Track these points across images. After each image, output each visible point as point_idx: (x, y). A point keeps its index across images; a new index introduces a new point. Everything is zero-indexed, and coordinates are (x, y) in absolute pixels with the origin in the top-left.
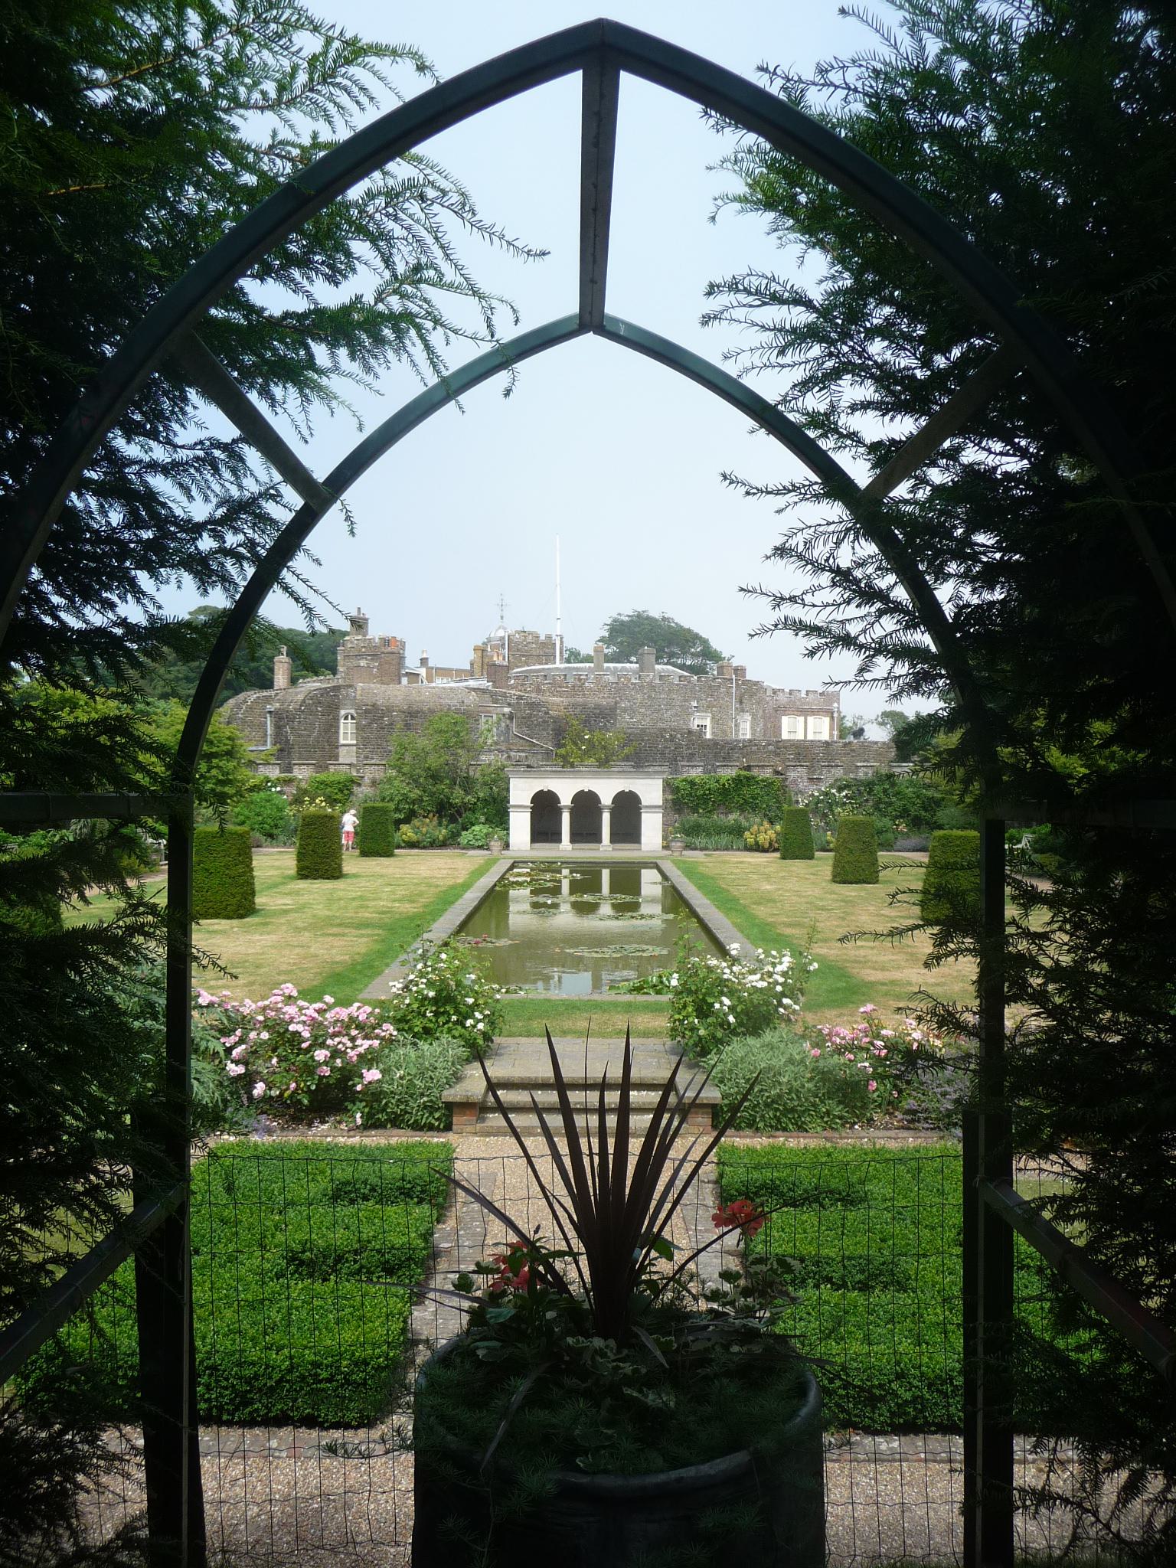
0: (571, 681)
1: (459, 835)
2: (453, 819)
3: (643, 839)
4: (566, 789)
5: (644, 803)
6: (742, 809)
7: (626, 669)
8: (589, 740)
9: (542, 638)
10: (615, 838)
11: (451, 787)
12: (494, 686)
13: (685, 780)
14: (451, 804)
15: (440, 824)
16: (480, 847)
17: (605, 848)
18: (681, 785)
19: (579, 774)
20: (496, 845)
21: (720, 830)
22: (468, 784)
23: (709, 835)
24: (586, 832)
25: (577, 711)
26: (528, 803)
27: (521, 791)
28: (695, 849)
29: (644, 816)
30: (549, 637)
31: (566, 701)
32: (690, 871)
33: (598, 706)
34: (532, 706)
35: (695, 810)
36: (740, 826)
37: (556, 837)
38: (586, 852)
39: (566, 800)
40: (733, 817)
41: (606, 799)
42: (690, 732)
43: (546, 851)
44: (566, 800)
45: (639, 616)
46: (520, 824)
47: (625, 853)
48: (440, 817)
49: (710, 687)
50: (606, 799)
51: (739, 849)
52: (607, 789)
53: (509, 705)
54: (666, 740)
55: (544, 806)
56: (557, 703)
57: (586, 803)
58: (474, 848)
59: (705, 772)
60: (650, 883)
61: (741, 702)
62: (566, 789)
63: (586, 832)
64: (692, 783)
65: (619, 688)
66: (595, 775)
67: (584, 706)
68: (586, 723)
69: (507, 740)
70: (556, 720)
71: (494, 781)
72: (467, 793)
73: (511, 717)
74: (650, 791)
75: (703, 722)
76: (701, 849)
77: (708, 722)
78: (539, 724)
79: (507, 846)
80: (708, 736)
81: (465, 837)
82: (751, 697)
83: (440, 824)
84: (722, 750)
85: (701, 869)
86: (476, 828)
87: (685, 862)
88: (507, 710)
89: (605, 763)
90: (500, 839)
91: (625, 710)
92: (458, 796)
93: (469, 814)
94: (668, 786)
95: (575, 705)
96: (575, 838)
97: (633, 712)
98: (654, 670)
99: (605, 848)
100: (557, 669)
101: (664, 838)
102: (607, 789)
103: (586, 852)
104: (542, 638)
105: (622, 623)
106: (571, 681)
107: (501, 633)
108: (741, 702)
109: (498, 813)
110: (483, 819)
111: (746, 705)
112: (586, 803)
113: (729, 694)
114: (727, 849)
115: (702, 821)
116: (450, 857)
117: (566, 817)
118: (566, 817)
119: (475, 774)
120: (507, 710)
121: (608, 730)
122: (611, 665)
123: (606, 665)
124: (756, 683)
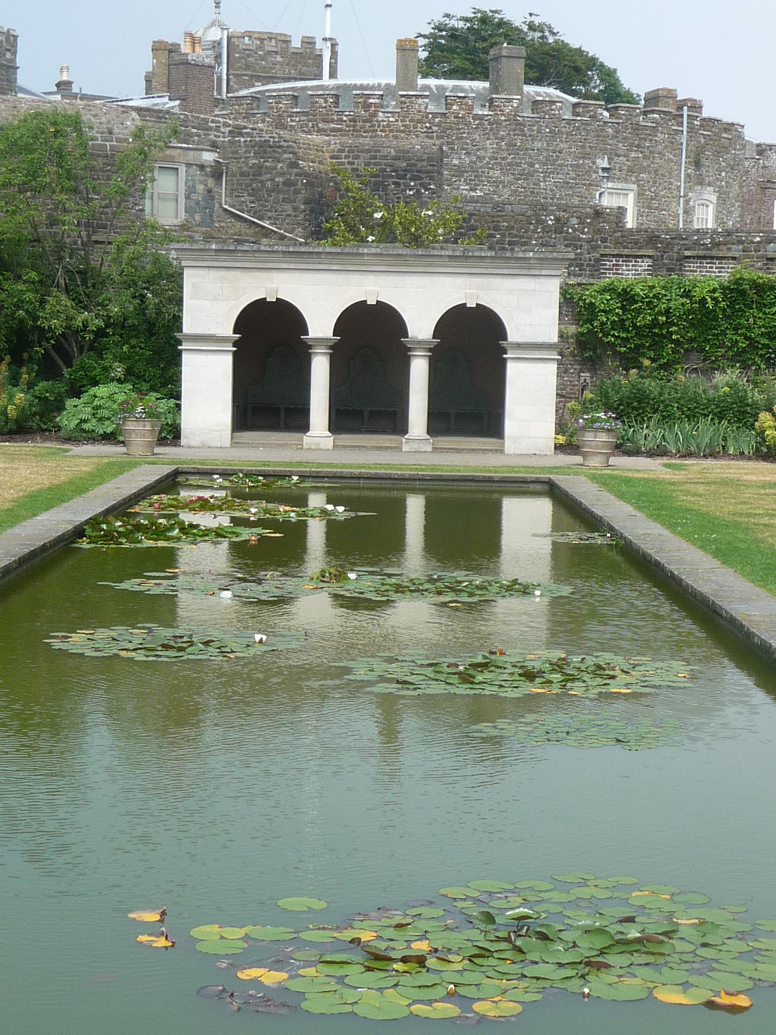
0: (348, 109)
1: (60, 408)
2: (48, 370)
3: (510, 426)
4: (321, 299)
5: (514, 334)
6: (741, 359)
7: (462, 90)
8: (385, 224)
9: (296, 43)
10: (439, 423)
11: (44, 285)
12: (182, 107)
13: (610, 289)
14: (41, 330)
15: (14, 380)
16: (109, 438)
17: (416, 445)
18: (601, 301)
19: (348, 262)
20: (140, 431)
21: (693, 410)
22: (85, 285)
23: (667, 418)
24: (368, 404)
25: (360, 164)
26: (227, 329)
27: (211, 302)
28: (636, 453)
29: (512, 369)
30: (309, 42)
31: (335, 142)
32: (653, 501)
33: (402, 154)
34: (263, 149)
35: (629, 361)
36: (742, 400)
37: (298, 420)
38: (368, 454)
39: (321, 324)
40: (726, 380)
41: (421, 325)
42: (598, 213)
43: (268, 450)
44: (321, 324)
45: (485, 20)
46: (207, 386)
47: (465, 457)
48: (17, 362)
49: (637, 127)
50: (421, 325)
51: (741, 455)
52: (422, 301)
53: (214, 146)
54: (547, 229)
55: (268, 337)
56: (319, 148)
57: (370, 333)
58: (92, 438)
59: (655, 270)
60: (526, 527)
61: (697, 164)
62: (321, 299)
63: (368, 404)
64: (626, 297)
65: (451, 122)
66: (397, 264)
67: (374, 153)
68: (378, 185)
69: (209, 220)
70: (313, 180)
71: (150, 281)
72: (81, 305)
73: (217, 173)
74: (530, 307)
75: (622, 200)
76: (651, 454)
77: (629, 203)
78: (275, 189)
79: (171, 434)
80: (630, 222)
81: (75, 412)
82: (717, 154)
83: (14, 380)
84: (670, 248)
85: (683, 500)
86: (102, 391)
87: (628, 481)
88: (208, 157)
89: (410, 243)
90: (151, 414)
91: (459, 172)
92: (59, 312)
93: (88, 359)
94: (570, 303)
95: (354, 151)
96: (343, 419)
97: (475, 176)
98: (522, 94)
99: (416, 445)
100: (321, 87)
101: (560, 428)
102: (422, 301)
103: (368, 454)
104: (296, 43)
105: (454, 34)
106: (348, 109)
107: (215, 34)
108: (697, 164)
109: (155, 355)
110: (119, 370)
111: (709, 171)
112: (370, 333)
113: (675, 146)
114: (713, 455)
115: (651, 386)
116: (12, 457)
117: (320, 369)
118: (320, 369)
119: (104, 261)
120: (208, 157)
121: (424, 205)
122: (432, 82)
123: (421, 82)
124: (729, 127)
